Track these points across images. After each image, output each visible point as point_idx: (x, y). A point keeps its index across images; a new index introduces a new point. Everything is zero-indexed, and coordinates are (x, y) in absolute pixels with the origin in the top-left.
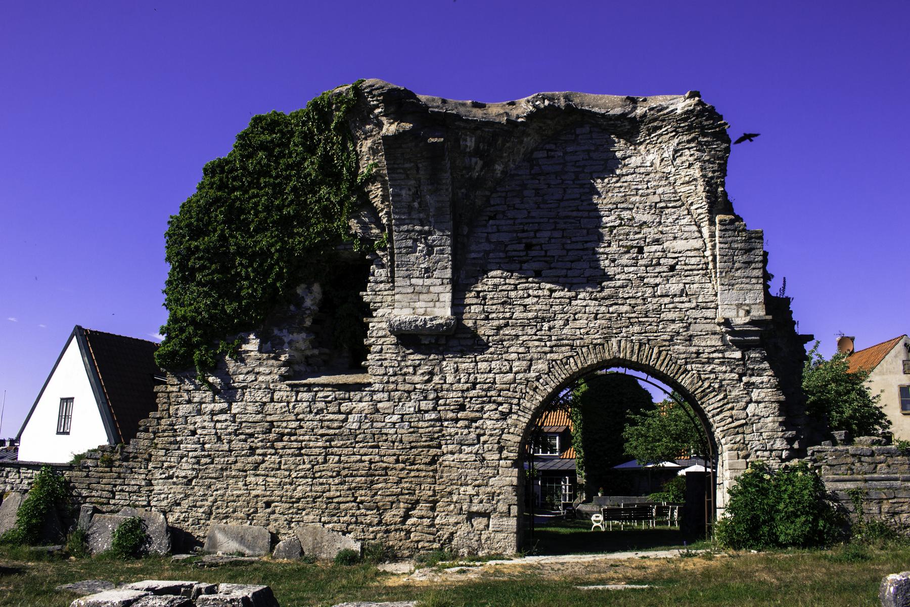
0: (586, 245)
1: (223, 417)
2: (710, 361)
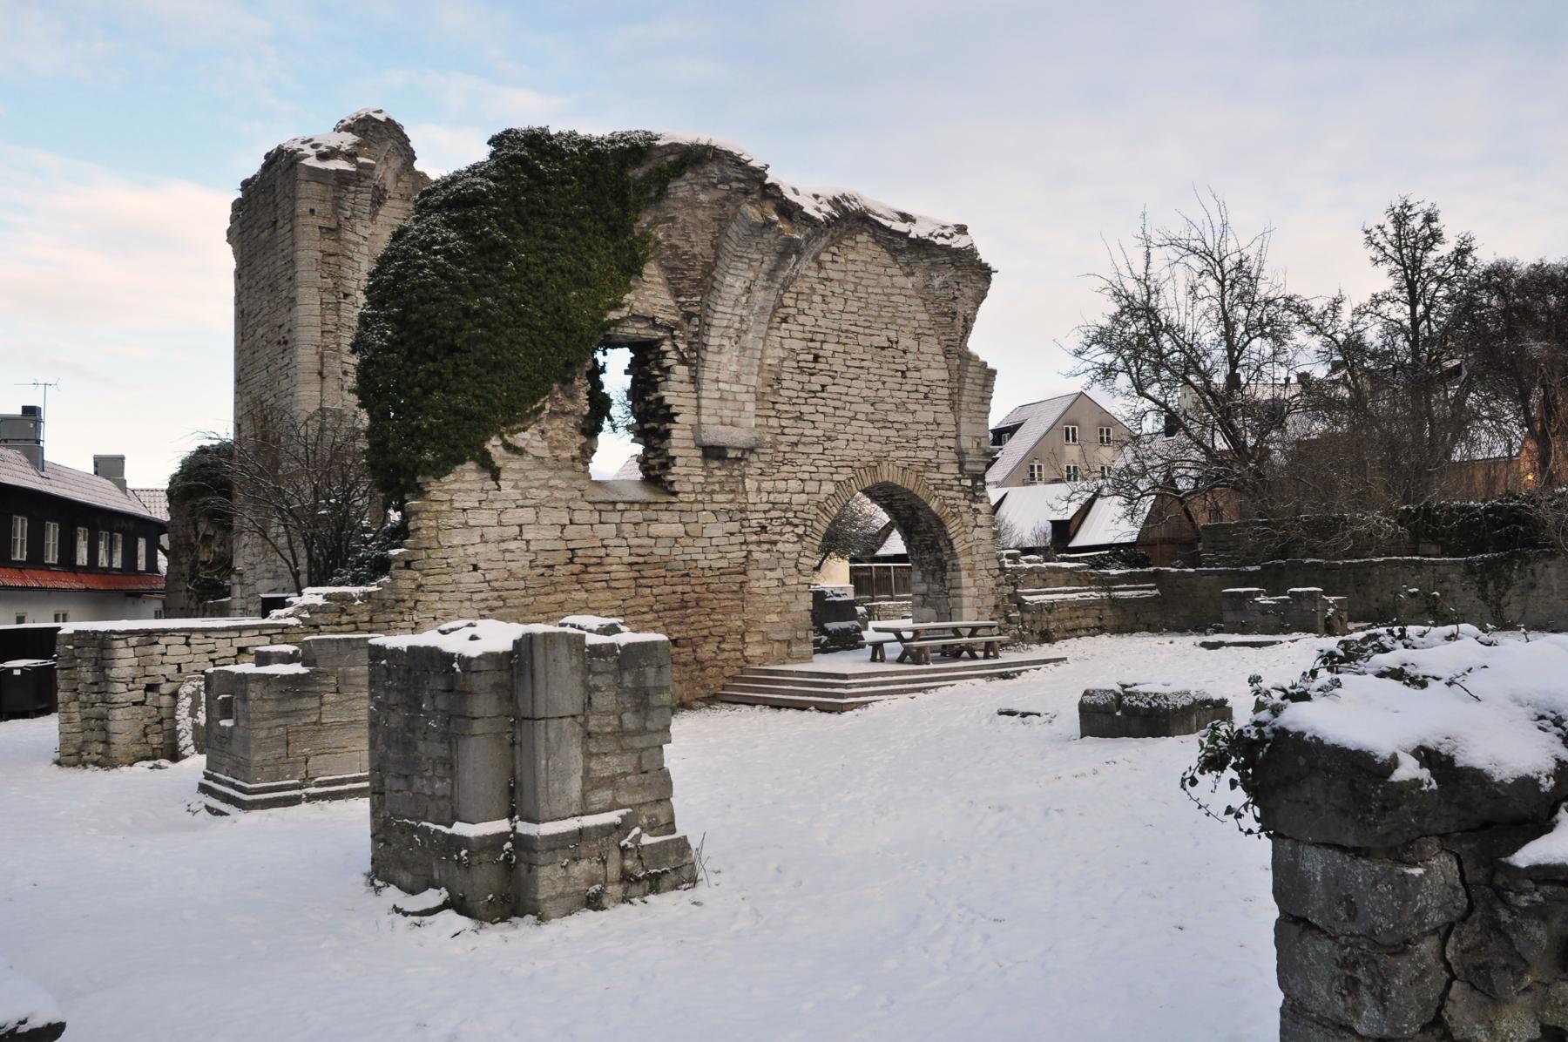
0: (864, 364)
1: (513, 545)
2: (951, 488)
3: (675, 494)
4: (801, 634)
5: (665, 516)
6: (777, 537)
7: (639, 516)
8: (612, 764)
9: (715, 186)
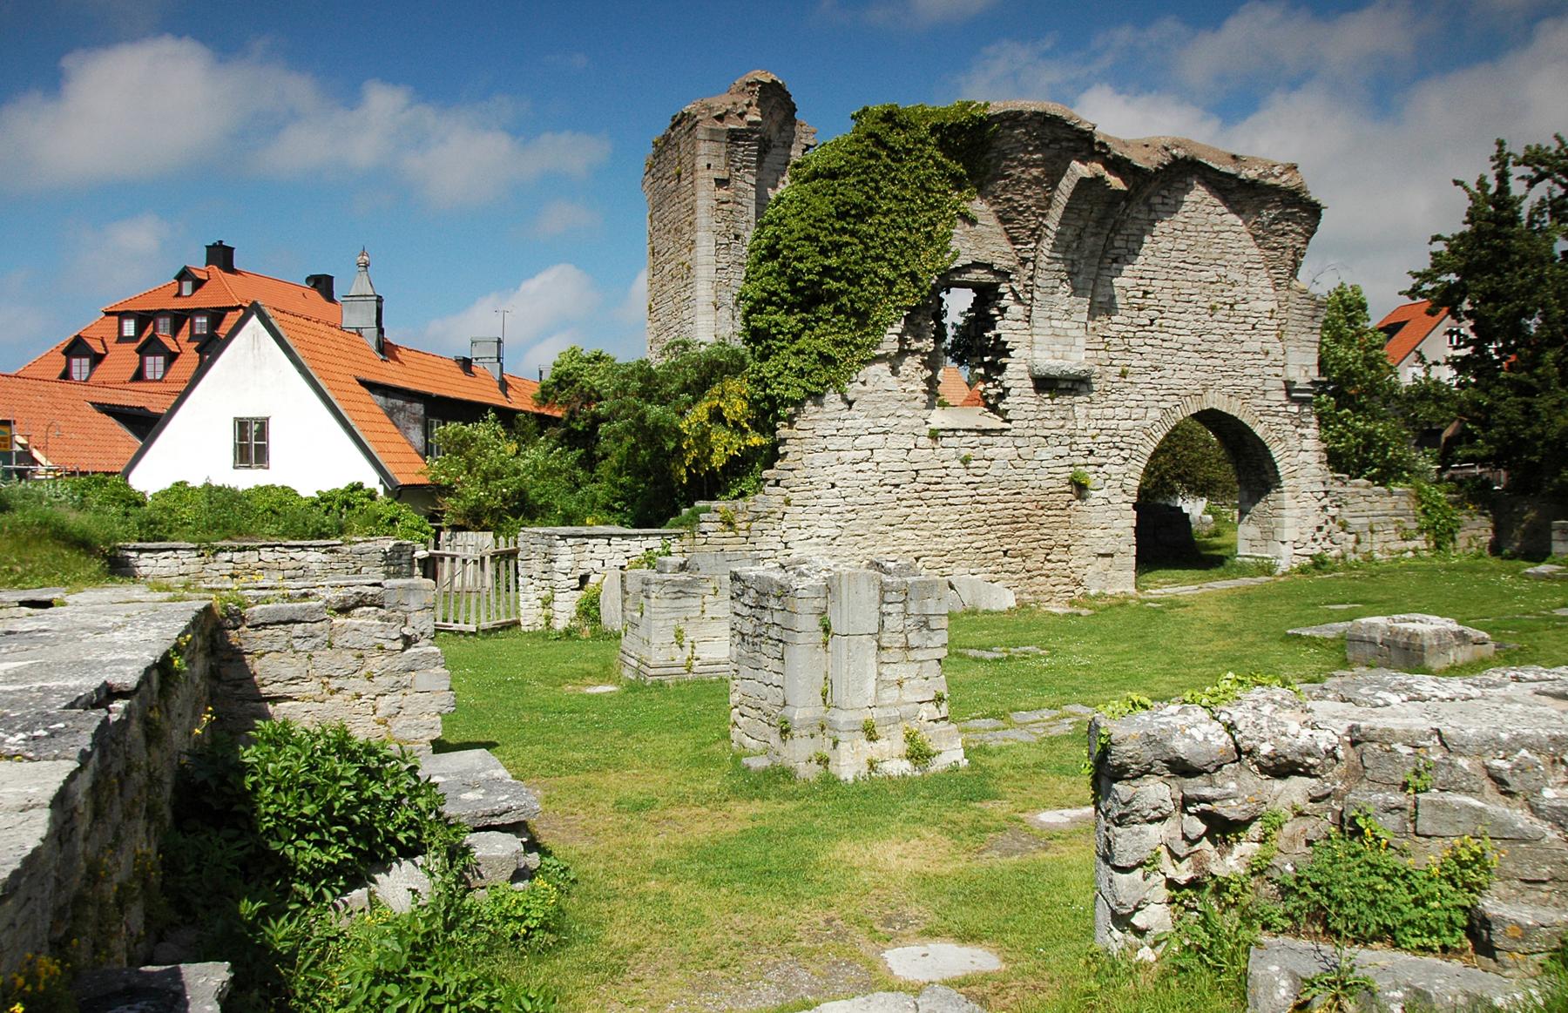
1: (864, 466)
2: (1277, 414)
3: (1010, 421)
4: (1123, 547)
5: (999, 440)
6: (1103, 460)
7: (977, 440)
8: (901, 671)
9: (1047, 146)
